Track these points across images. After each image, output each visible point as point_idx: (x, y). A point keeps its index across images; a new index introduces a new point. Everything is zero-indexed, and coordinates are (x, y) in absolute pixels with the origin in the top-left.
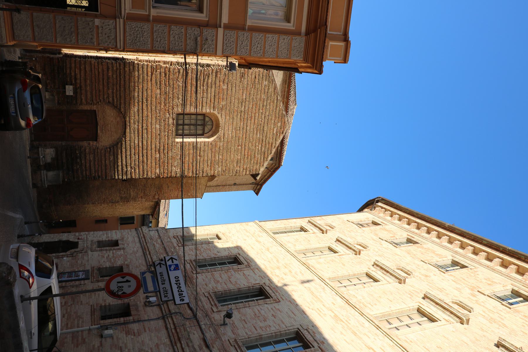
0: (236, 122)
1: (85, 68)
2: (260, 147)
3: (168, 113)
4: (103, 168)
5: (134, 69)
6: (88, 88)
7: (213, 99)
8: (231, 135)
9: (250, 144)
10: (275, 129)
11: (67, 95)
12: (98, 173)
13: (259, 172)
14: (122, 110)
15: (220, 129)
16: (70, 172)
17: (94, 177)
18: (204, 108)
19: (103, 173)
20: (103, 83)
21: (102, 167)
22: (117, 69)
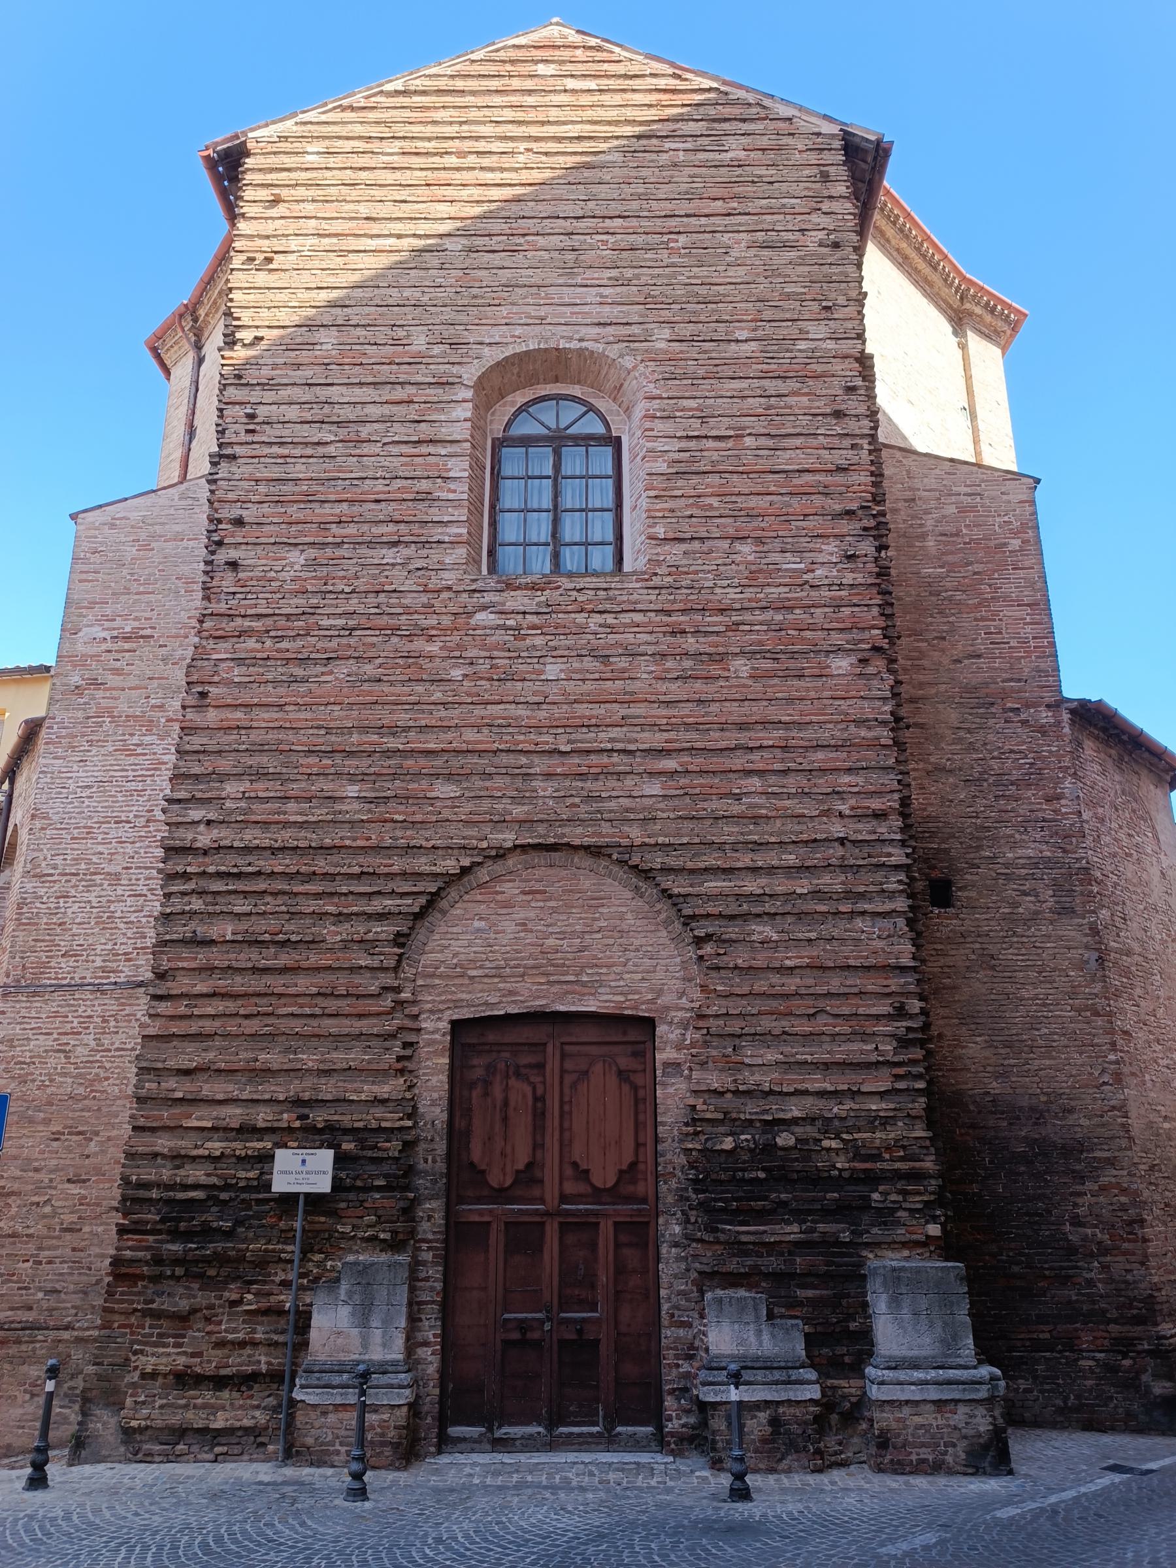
0: (530, 272)
1: (187, 1072)
2: (674, 146)
3: (470, 615)
4: (835, 983)
5: (209, 800)
6: (309, 1059)
7: (400, 393)
8: (606, 291)
9: (663, 191)
10: (571, 84)
11: (333, 1188)
12: (878, 1017)
13: (833, 136)
14: (450, 865)
15: (574, 345)
16: (876, 1196)
17: (903, 1043)
18: (444, 432)
19: (870, 988)
20: (285, 970)
21: (829, 995)
22: (201, 893)
